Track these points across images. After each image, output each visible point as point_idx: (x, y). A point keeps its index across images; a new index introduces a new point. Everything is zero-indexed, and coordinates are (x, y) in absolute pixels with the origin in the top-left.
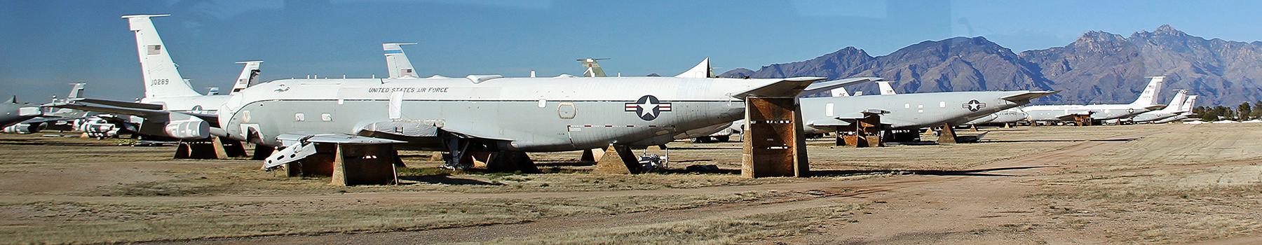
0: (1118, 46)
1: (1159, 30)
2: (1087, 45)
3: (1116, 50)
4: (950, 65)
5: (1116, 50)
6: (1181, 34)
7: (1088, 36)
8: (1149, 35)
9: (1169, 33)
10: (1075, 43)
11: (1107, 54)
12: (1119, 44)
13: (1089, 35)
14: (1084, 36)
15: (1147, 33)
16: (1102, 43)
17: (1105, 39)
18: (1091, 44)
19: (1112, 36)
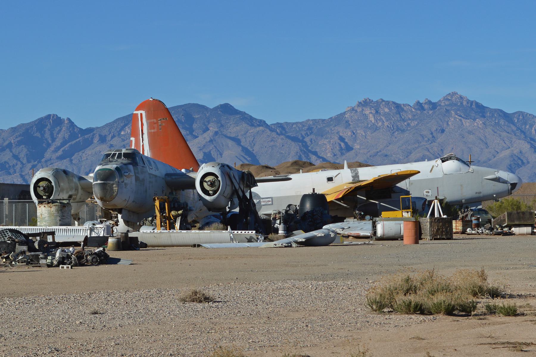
0: (410, 119)
1: (445, 99)
2: (366, 117)
3: (408, 124)
4: (211, 141)
5: (408, 124)
7: (363, 105)
8: (434, 106)
9: (462, 103)
10: (345, 113)
11: (398, 129)
12: (410, 117)
13: (366, 103)
14: (358, 106)
15: (430, 102)
16: (386, 115)
17: (390, 109)
18: (371, 115)
19: (398, 106)
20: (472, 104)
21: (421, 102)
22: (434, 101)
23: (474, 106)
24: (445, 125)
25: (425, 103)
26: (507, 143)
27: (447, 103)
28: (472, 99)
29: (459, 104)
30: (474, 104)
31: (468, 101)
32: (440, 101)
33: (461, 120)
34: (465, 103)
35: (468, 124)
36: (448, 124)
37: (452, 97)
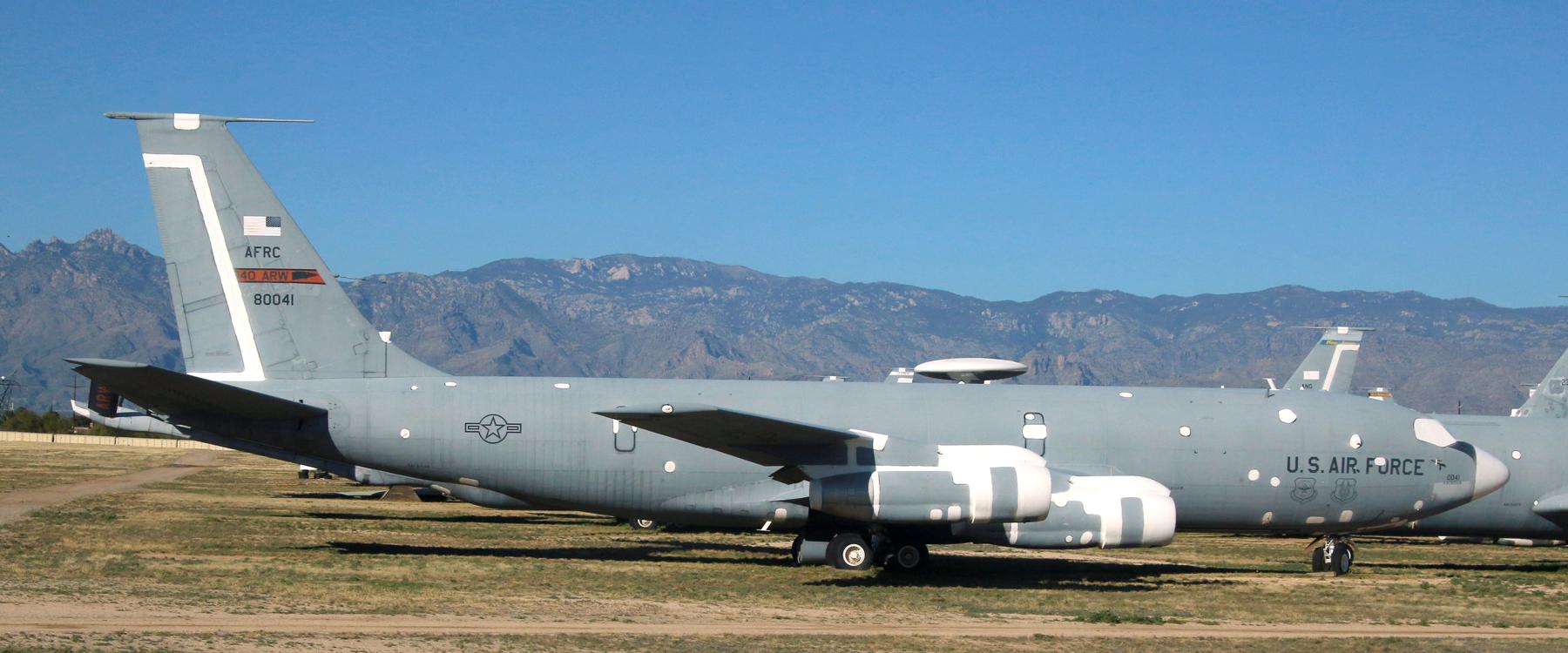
1: (89, 240)
6: (138, 252)
8: (65, 249)
9: (110, 247)
15: (60, 244)
20: (127, 252)
21: (43, 241)
22: (69, 239)
23: (131, 254)
24: (45, 281)
25: (51, 244)
26: (124, 314)
27: (88, 245)
28: (131, 241)
29: (106, 248)
30: (131, 250)
31: (124, 243)
32: (79, 243)
33: (71, 274)
34: (115, 248)
35: (80, 281)
36: (50, 280)
37: (98, 237)
